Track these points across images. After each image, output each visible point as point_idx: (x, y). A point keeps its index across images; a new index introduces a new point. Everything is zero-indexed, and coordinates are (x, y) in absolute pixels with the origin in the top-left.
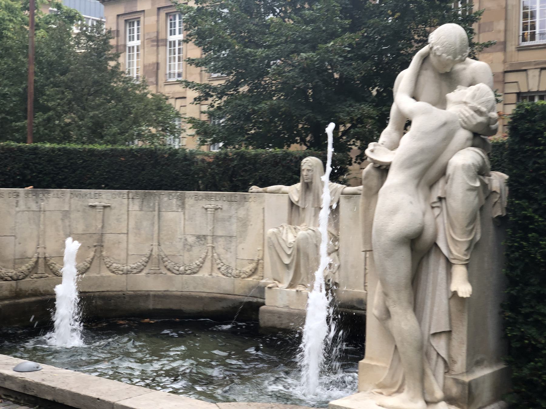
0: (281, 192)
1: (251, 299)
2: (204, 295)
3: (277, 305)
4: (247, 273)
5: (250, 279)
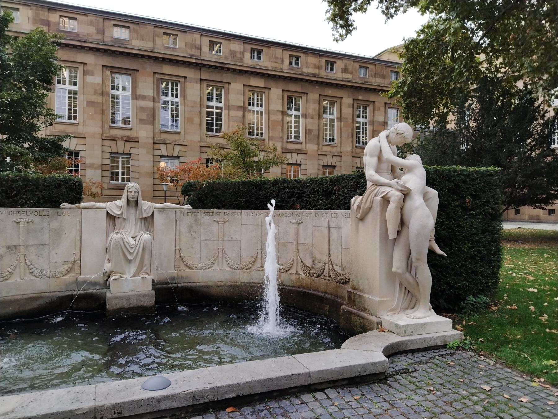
0: (94, 207)
1: (70, 293)
2: (19, 297)
3: (123, 291)
4: (63, 273)
5: (67, 277)
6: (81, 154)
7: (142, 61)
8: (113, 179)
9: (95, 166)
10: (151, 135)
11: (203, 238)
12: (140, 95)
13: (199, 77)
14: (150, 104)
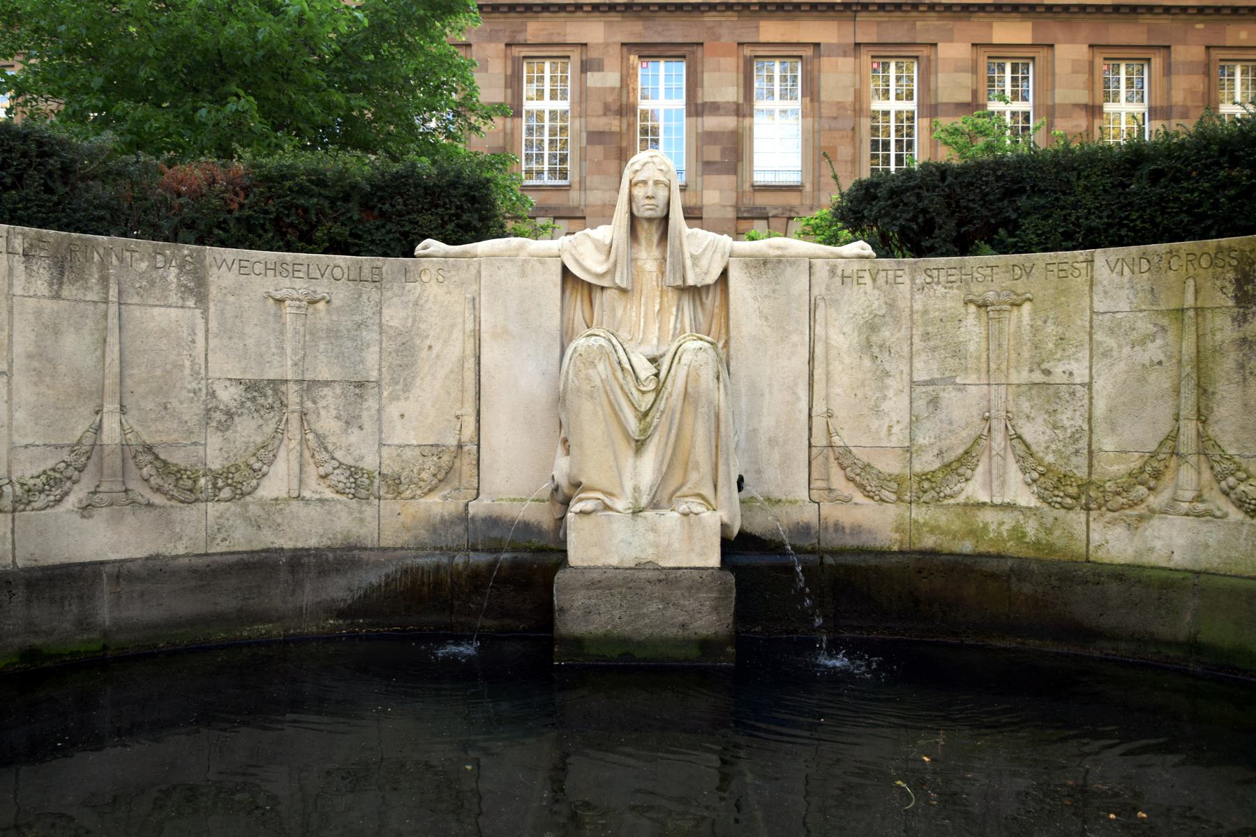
4: (421, 484)
7: (710, 18)
10: (731, 198)
11: (921, 376)
12: (704, 104)
13: (850, 40)
14: (730, 122)
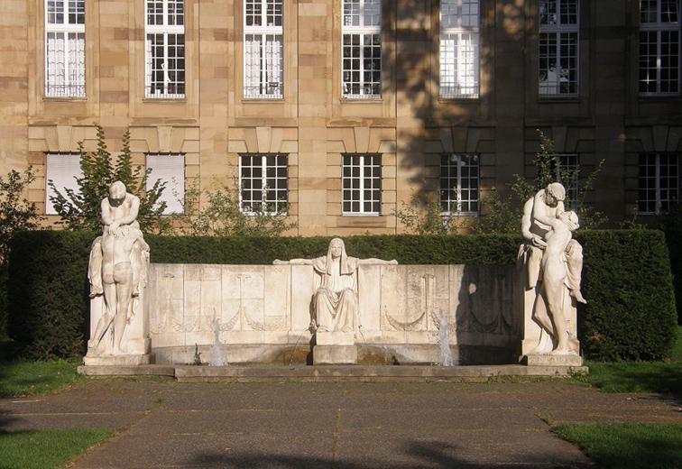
6: (292, 160)
8: (347, 207)
9: (314, 183)
